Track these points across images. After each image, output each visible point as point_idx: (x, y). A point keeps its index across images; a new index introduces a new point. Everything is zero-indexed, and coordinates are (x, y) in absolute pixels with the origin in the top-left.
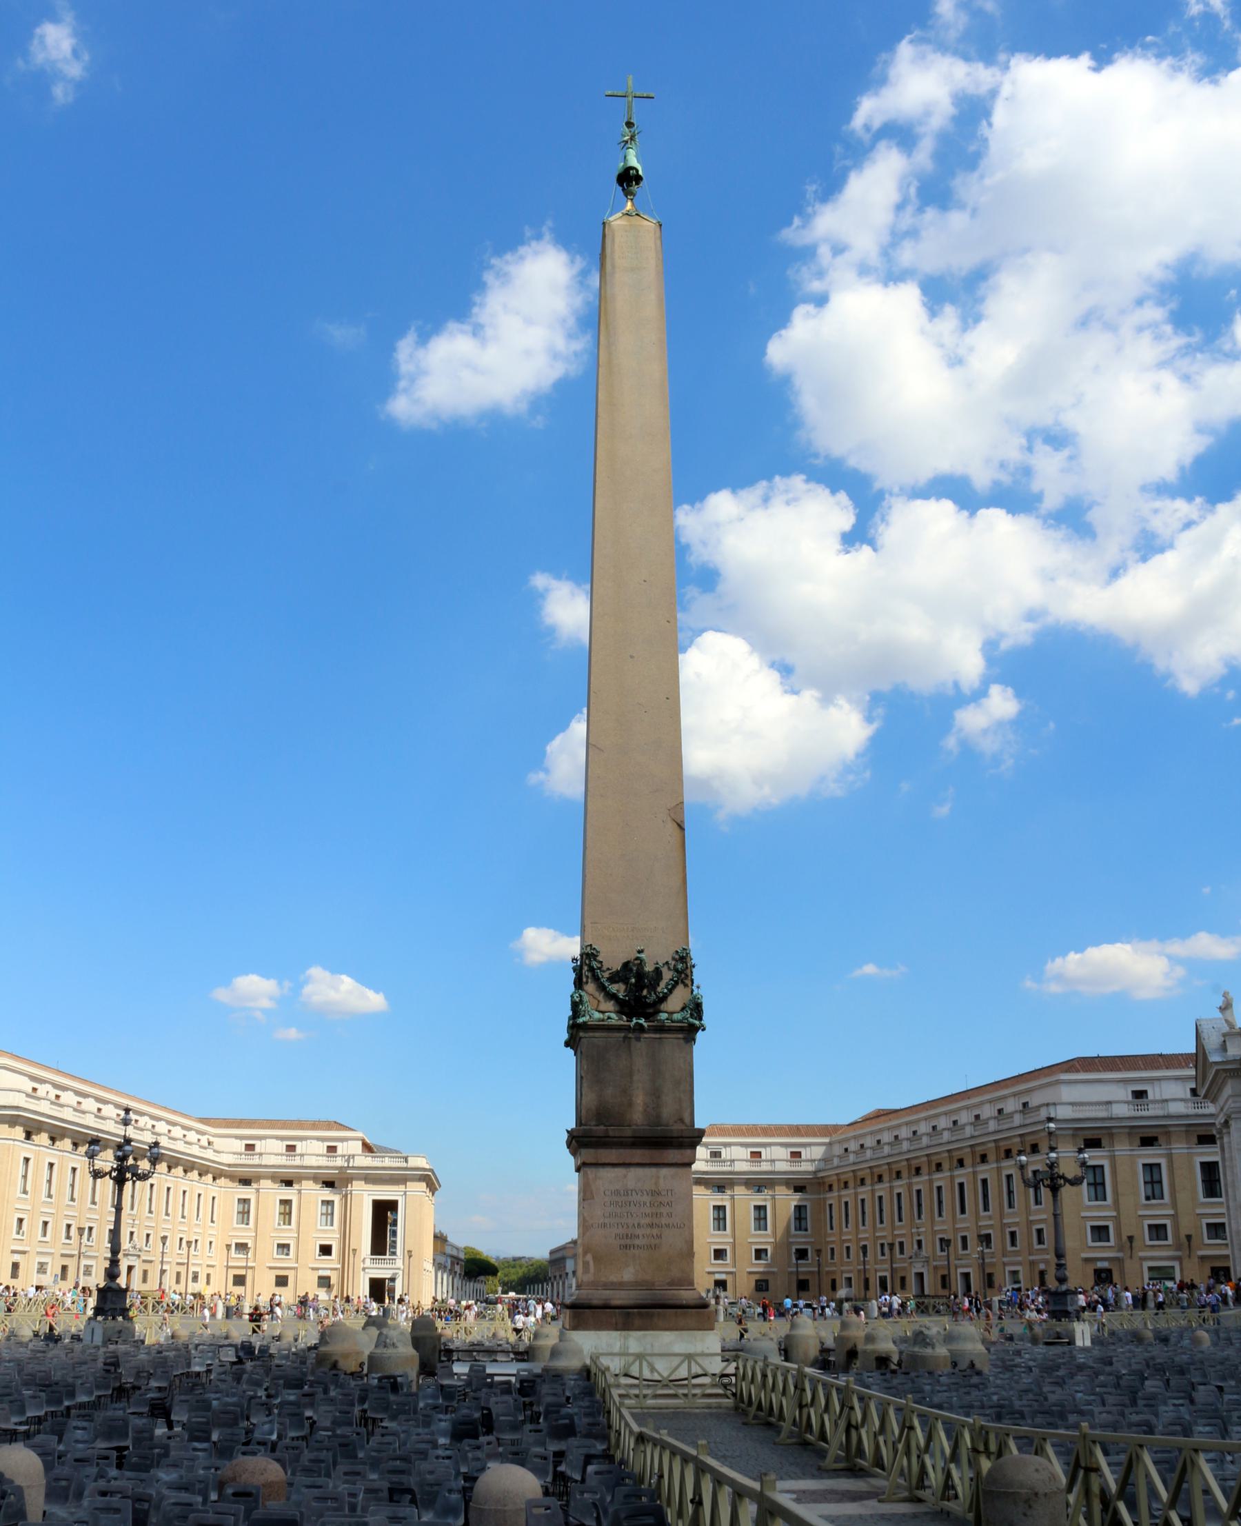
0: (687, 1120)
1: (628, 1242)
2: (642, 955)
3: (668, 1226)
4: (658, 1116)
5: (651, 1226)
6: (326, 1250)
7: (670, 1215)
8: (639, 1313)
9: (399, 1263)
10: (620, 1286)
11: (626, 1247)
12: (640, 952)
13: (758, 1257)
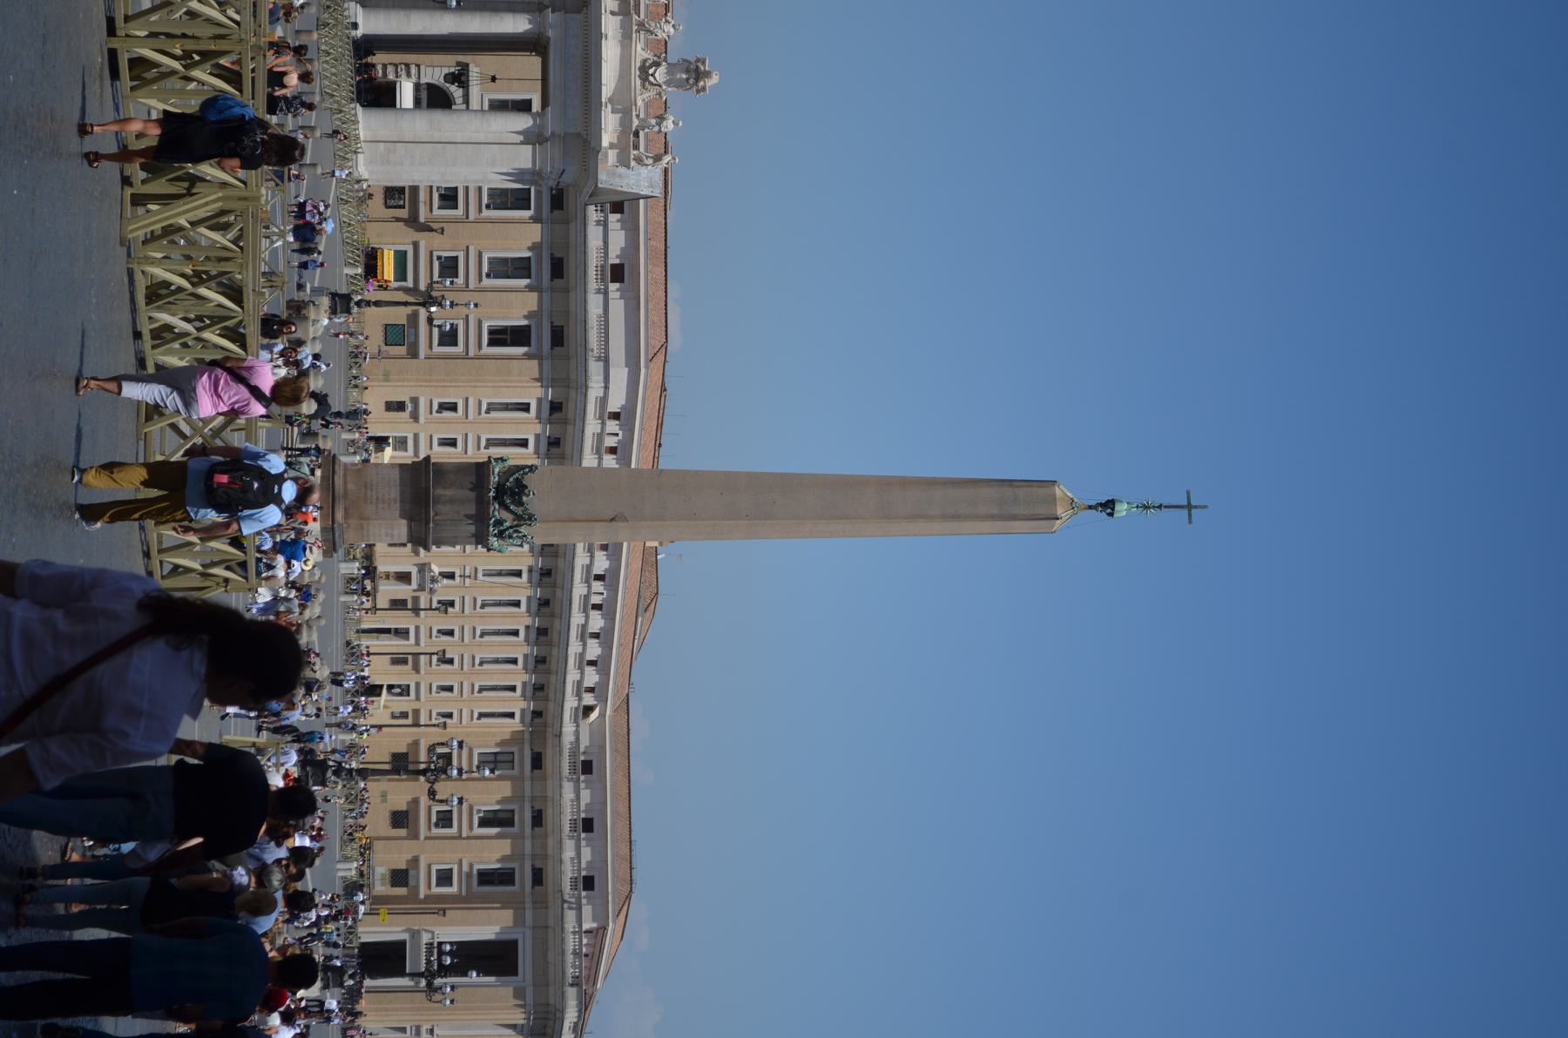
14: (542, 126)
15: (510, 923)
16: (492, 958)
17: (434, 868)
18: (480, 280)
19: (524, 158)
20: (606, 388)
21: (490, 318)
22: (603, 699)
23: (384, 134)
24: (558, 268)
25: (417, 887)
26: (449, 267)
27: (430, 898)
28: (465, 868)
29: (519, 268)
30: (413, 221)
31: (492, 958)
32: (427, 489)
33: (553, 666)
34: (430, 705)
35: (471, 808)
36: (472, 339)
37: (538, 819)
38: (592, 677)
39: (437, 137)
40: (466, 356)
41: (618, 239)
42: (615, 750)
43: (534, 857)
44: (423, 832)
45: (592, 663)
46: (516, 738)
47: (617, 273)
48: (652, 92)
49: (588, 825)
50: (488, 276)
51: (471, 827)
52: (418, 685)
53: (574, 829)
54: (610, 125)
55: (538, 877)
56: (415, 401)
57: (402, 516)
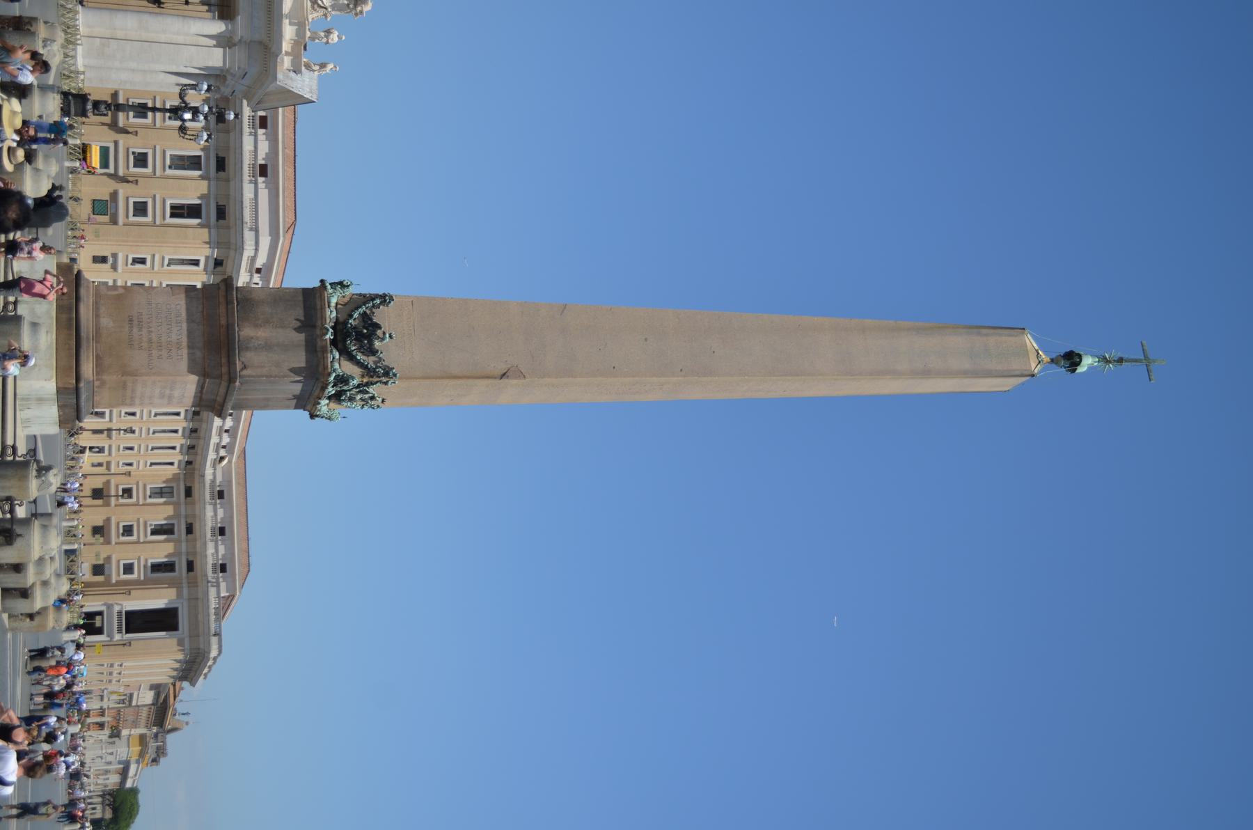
0: (245, 372)
1: (135, 322)
2: (388, 339)
3: (150, 355)
4: (247, 349)
5: (150, 341)
6: (129, 569)
7: (160, 357)
8: (70, 319)
9: (117, 637)
10: (97, 316)
11: (131, 321)
12: (391, 337)
13: (125, 491)
14: (233, 32)
15: (174, 597)
16: (162, 620)
17: (122, 563)
18: (164, 170)
19: (215, 58)
20: (256, 250)
21: (171, 198)
22: (231, 452)
23: (98, 31)
24: (221, 164)
25: (110, 576)
26: (141, 160)
27: (119, 583)
28: (142, 563)
29: (194, 163)
30: (114, 126)
31: (162, 620)
32: (229, 328)
33: (202, 434)
34: (117, 460)
35: (145, 523)
36: (159, 212)
37: (190, 530)
38: (226, 439)
39: (144, 36)
40: (154, 224)
41: (264, 147)
42: (238, 483)
43: (188, 553)
44: (114, 539)
45: (227, 431)
46: (175, 478)
47: (263, 170)
48: (322, 11)
49: (222, 531)
50: (170, 167)
51: (146, 536)
52: (110, 447)
53: (213, 535)
54: (289, 32)
55: (190, 566)
56: (115, 256)
57: (191, 370)
